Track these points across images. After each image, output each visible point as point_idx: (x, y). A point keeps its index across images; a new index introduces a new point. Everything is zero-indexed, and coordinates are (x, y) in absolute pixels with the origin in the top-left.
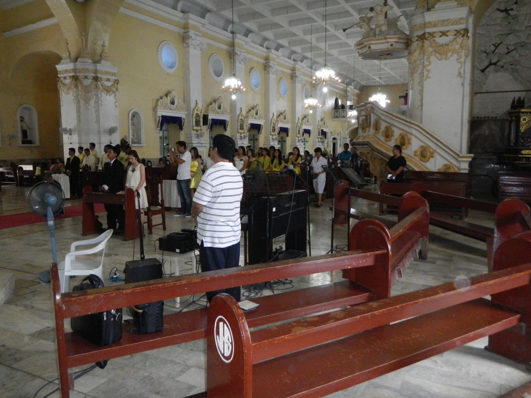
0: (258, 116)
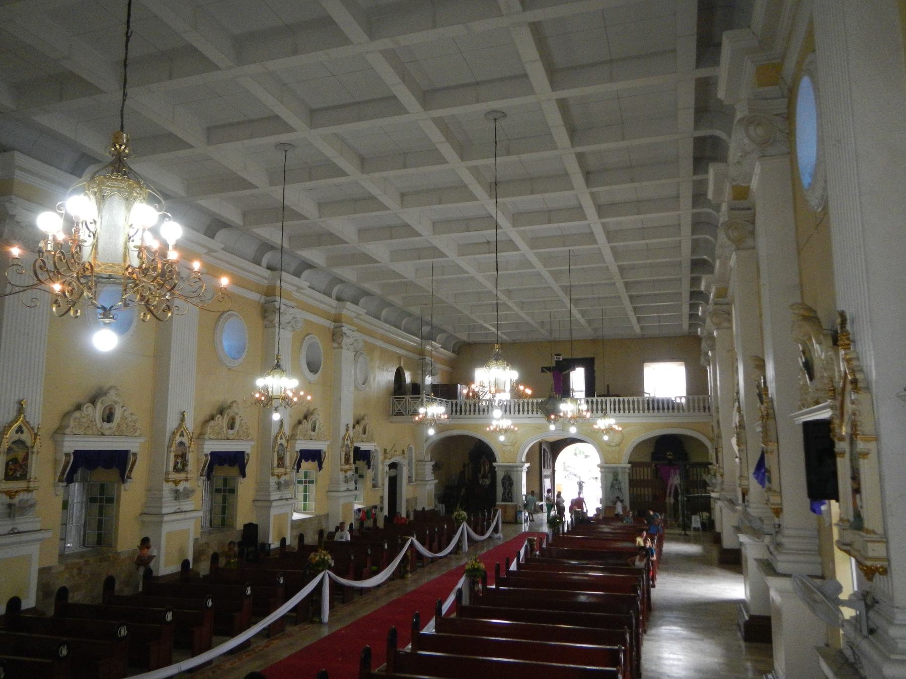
0: (114, 425)
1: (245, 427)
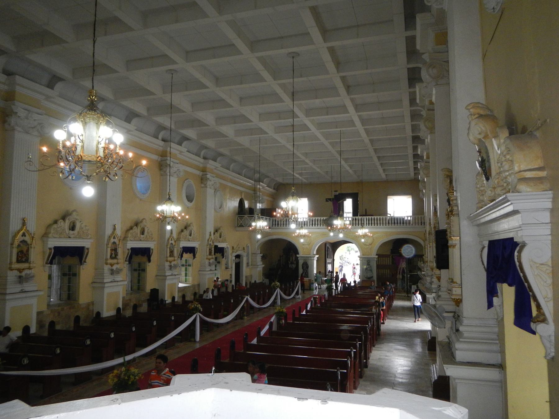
0: (76, 232)
1: (150, 233)
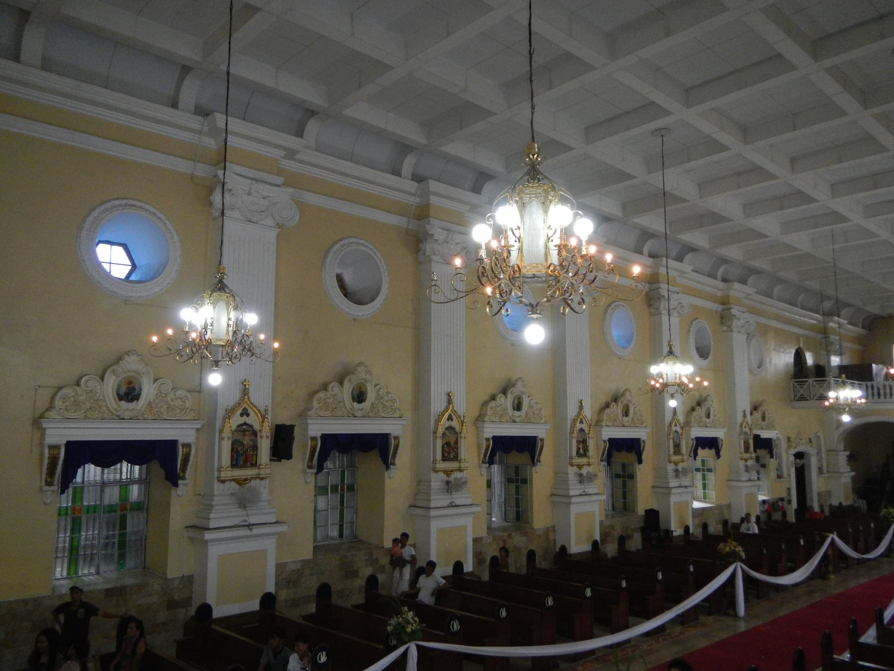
0: (522, 413)
1: (639, 414)
